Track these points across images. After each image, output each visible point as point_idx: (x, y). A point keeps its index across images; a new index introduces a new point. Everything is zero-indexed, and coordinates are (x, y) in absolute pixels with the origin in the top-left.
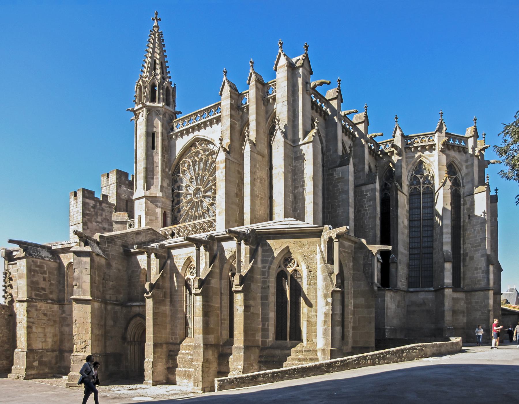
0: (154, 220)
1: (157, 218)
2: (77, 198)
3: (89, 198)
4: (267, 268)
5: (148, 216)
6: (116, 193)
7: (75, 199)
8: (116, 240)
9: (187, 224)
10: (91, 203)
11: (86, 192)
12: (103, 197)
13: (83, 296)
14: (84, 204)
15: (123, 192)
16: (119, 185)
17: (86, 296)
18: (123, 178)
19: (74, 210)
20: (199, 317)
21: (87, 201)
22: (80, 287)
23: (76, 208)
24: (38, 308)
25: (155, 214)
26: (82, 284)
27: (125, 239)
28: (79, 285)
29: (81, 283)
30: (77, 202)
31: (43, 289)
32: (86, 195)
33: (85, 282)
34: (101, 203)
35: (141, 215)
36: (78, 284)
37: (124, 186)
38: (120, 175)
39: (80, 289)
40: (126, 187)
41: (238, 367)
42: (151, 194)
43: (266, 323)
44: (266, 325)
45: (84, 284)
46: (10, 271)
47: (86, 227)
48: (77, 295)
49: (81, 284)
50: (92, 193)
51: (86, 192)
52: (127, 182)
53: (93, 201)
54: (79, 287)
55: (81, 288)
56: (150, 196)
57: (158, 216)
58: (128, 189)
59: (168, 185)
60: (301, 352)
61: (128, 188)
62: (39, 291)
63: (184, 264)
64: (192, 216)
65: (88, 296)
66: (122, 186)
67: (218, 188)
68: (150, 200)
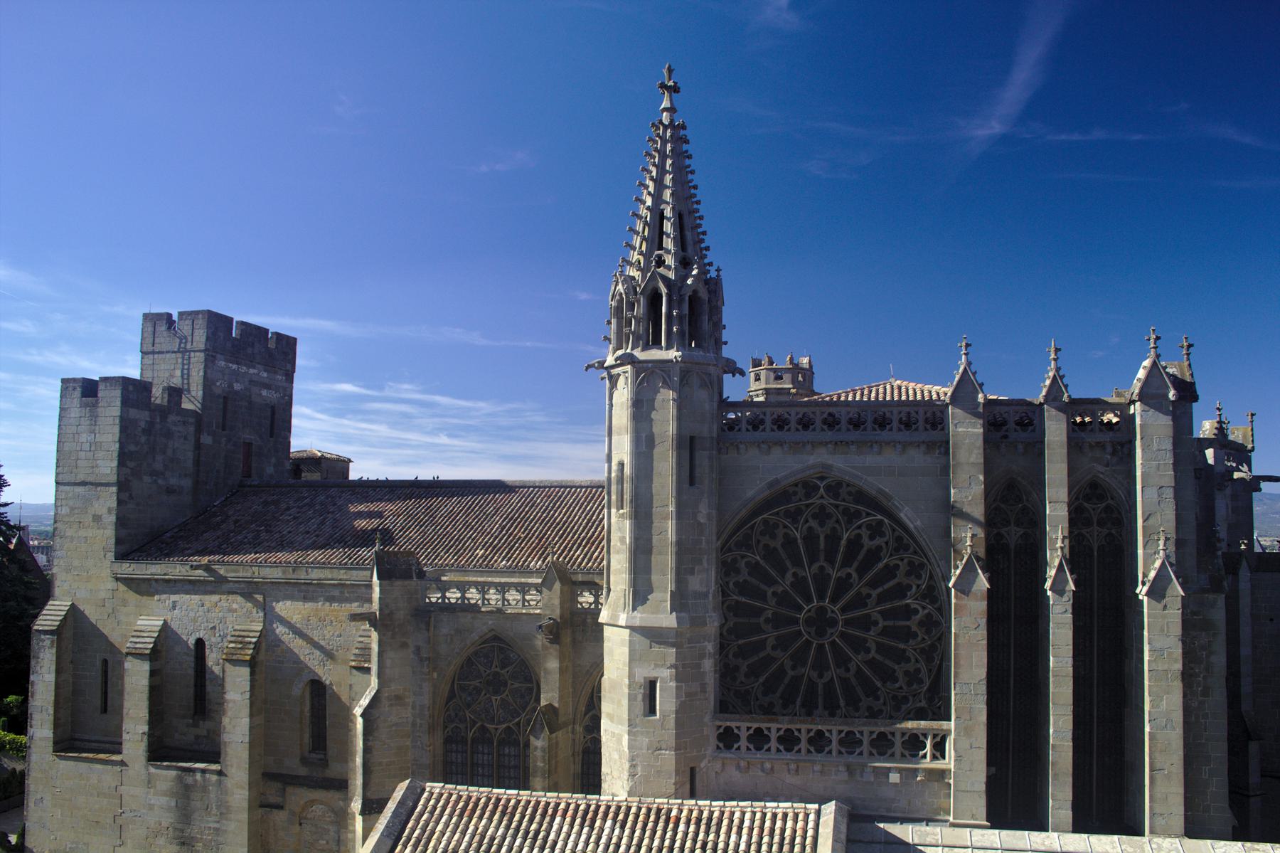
2: (97, 402)
5: (683, 684)
10: (142, 416)
12: (170, 395)
16: (212, 356)
19: (84, 437)
21: (133, 413)
30: (94, 417)
32: (131, 396)
34: (163, 412)
35: (657, 678)
37: (222, 357)
40: (225, 360)
51: (131, 388)
52: (229, 345)
53: (147, 413)
58: (231, 365)
61: (231, 363)
66: (219, 356)
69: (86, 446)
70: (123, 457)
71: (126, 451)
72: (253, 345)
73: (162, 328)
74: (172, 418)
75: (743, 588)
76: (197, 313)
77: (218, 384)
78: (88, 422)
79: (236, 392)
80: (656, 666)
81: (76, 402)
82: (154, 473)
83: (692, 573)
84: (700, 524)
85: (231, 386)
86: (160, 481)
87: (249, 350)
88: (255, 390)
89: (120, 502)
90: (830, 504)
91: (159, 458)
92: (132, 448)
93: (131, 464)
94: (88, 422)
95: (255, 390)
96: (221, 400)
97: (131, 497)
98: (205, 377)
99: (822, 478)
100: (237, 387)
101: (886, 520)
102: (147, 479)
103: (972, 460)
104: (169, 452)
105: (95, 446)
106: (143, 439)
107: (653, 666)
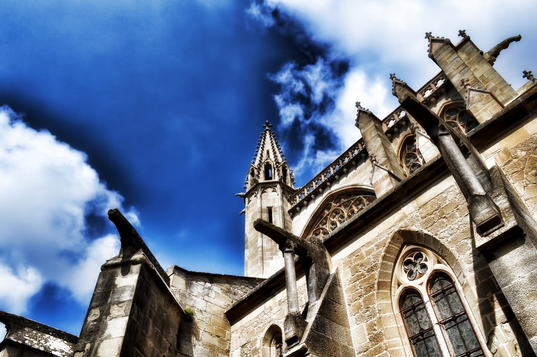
33: (109, 337)
63: (384, 258)
83: (272, 258)
90: (338, 207)
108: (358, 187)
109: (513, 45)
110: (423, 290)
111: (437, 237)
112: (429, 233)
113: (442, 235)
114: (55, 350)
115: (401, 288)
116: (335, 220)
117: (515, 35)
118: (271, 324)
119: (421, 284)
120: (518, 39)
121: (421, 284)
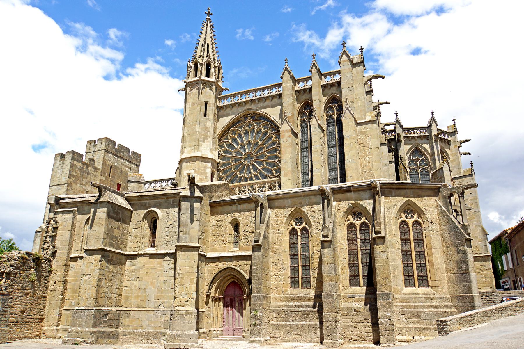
0: (203, 179)
1: (206, 177)
2: (64, 159)
3: (77, 161)
4: (392, 218)
6: (102, 159)
7: (61, 161)
8: (205, 190)
9: (234, 184)
11: (75, 154)
12: (90, 161)
13: (190, 242)
14: (72, 166)
15: (110, 159)
17: (193, 243)
18: (111, 146)
19: (59, 171)
20: (329, 265)
22: (188, 233)
23: (62, 169)
24: (110, 258)
25: (205, 174)
26: (189, 230)
27: (210, 190)
28: (186, 231)
29: (188, 230)
30: (63, 164)
31: (116, 238)
34: (87, 165)
35: (190, 173)
36: (185, 230)
38: (109, 143)
39: (187, 236)
41: (387, 314)
42: (202, 155)
43: (396, 270)
44: (396, 272)
45: (191, 230)
46: (57, 219)
47: (70, 188)
48: (183, 241)
49: (188, 230)
50: (81, 156)
51: (75, 154)
54: (185, 233)
55: (189, 234)
56: (201, 157)
57: (207, 175)
58: (114, 157)
59: (216, 149)
60: (435, 299)
62: (112, 240)
63: (290, 215)
64: (241, 178)
65: (195, 243)
67: (283, 153)
68: (201, 160)
69: (60, 173)
70: (70, 176)
71: (72, 174)
72: (123, 153)
73: (93, 144)
74: (90, 168)
75: (226, 151)
76: (103, 138)
77: (109, 161)
78: (61, 166)
79: (116, 166)
80: (190, 169)
81: (58, 160)
82: (82, 184)
83: (204, 141)
84: (207, 128)
85: (114, 163)
86: (84, 187)
87: (122, 154)
88: (123, 167)
89: (67, 190)
91: (84, 180)
92: (74, 174)
93: (73, 179)
94: (61, 166)
95: (123, 167)
96: (110, 167)
97: (72, 189)
98: (104, 158)
99: (249, 114)
100: (116, 164)
101: (268, 123)
102: (79, 185)
103: (289, 93)
104: (88, 179)
105: (62, 173)
106: (79, 172)
107: (189, 170)
108: (269, 116)
109: (380, 79)
110: (299, 231)
111: (309, 217)
112: (308, 214)
113: (311, 218)
114: (122, 204)
115: (291, 227)
116: (248, 129)
117: (383, 75)
118: (234, 218)
119: (299, 229)
120: (383, 78)
121: (299, 229)
